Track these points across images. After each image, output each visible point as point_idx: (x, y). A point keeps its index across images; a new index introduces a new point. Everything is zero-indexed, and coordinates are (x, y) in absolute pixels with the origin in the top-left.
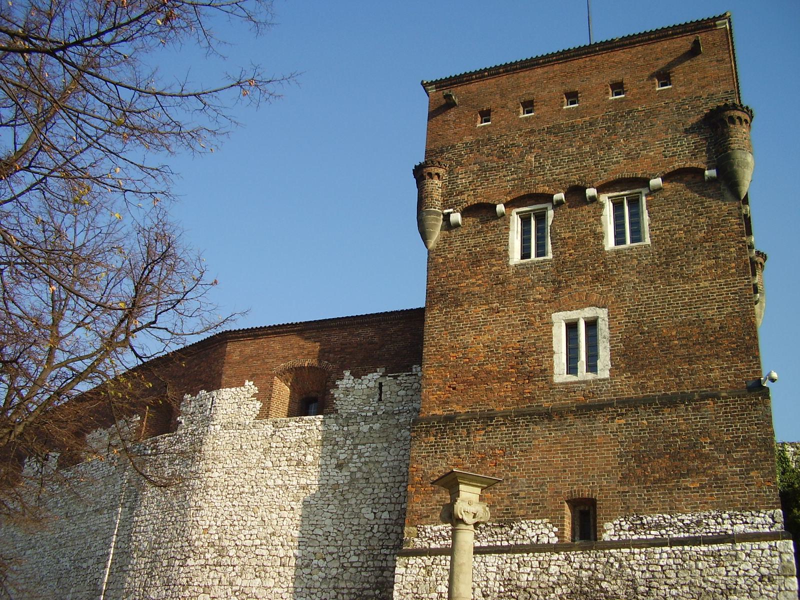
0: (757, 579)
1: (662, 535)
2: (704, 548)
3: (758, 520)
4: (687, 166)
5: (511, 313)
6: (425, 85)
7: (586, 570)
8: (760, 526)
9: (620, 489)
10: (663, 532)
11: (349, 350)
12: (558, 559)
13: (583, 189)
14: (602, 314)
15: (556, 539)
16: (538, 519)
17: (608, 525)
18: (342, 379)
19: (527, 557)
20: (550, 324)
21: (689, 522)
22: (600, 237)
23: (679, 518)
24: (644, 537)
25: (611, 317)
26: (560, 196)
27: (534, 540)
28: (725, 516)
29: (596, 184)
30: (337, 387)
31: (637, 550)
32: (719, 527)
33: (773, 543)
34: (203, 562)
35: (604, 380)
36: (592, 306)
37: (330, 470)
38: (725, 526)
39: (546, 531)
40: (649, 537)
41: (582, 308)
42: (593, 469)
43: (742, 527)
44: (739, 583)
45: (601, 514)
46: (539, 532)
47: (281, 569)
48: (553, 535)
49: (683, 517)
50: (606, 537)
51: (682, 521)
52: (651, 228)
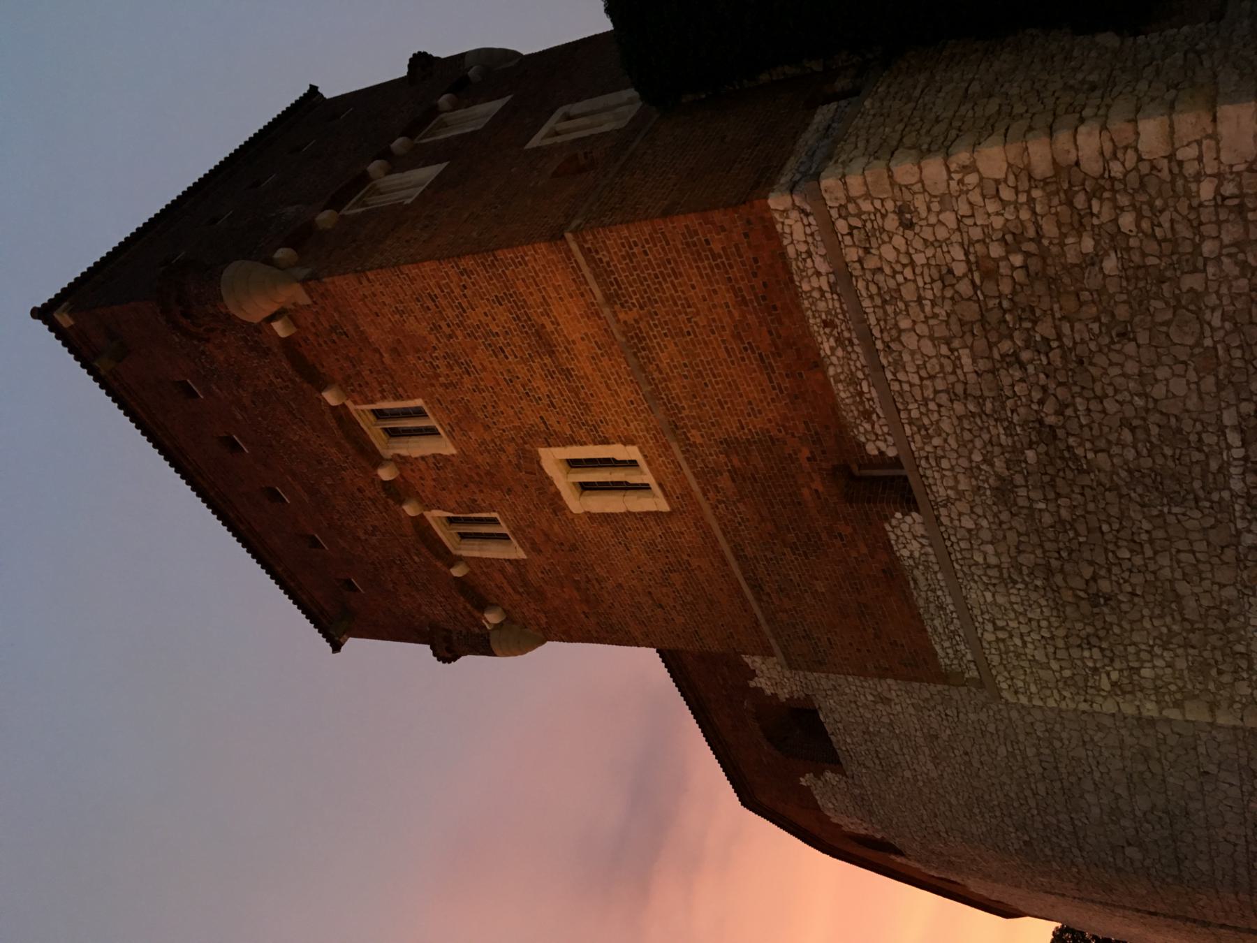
0: (909, 234)
1: (866, 377)
3: (799, 235)
6: (336, 648)
8: (808, 231)
10: (860, 375)
11: (721, 682)
12: (949, 516)
15: (914, 514)
16: (887, 535)
18: (762, 690)
21: (832, 340)
23: (829, 352)
24: (876, 400)
26: (410, 509)
27: (924, 541)
28: (806, 287)
30: (775, 695)
31: (903, 415)
32: (828, 295)
33: (834, 213)
34: (1076, 851)
35: (641, 450)
36: (541, 468)
37: (895, 712)
38: (826, 287)
39: (905, 527)
40: (874, 394)
41: (548, 478)
42: (784, 468)
43: (818, 260)
44: (924, 261)
46: (908, 536)
48: (908, 519)
49: (826, 346)
51: (832, 348)
52: (398, 397)
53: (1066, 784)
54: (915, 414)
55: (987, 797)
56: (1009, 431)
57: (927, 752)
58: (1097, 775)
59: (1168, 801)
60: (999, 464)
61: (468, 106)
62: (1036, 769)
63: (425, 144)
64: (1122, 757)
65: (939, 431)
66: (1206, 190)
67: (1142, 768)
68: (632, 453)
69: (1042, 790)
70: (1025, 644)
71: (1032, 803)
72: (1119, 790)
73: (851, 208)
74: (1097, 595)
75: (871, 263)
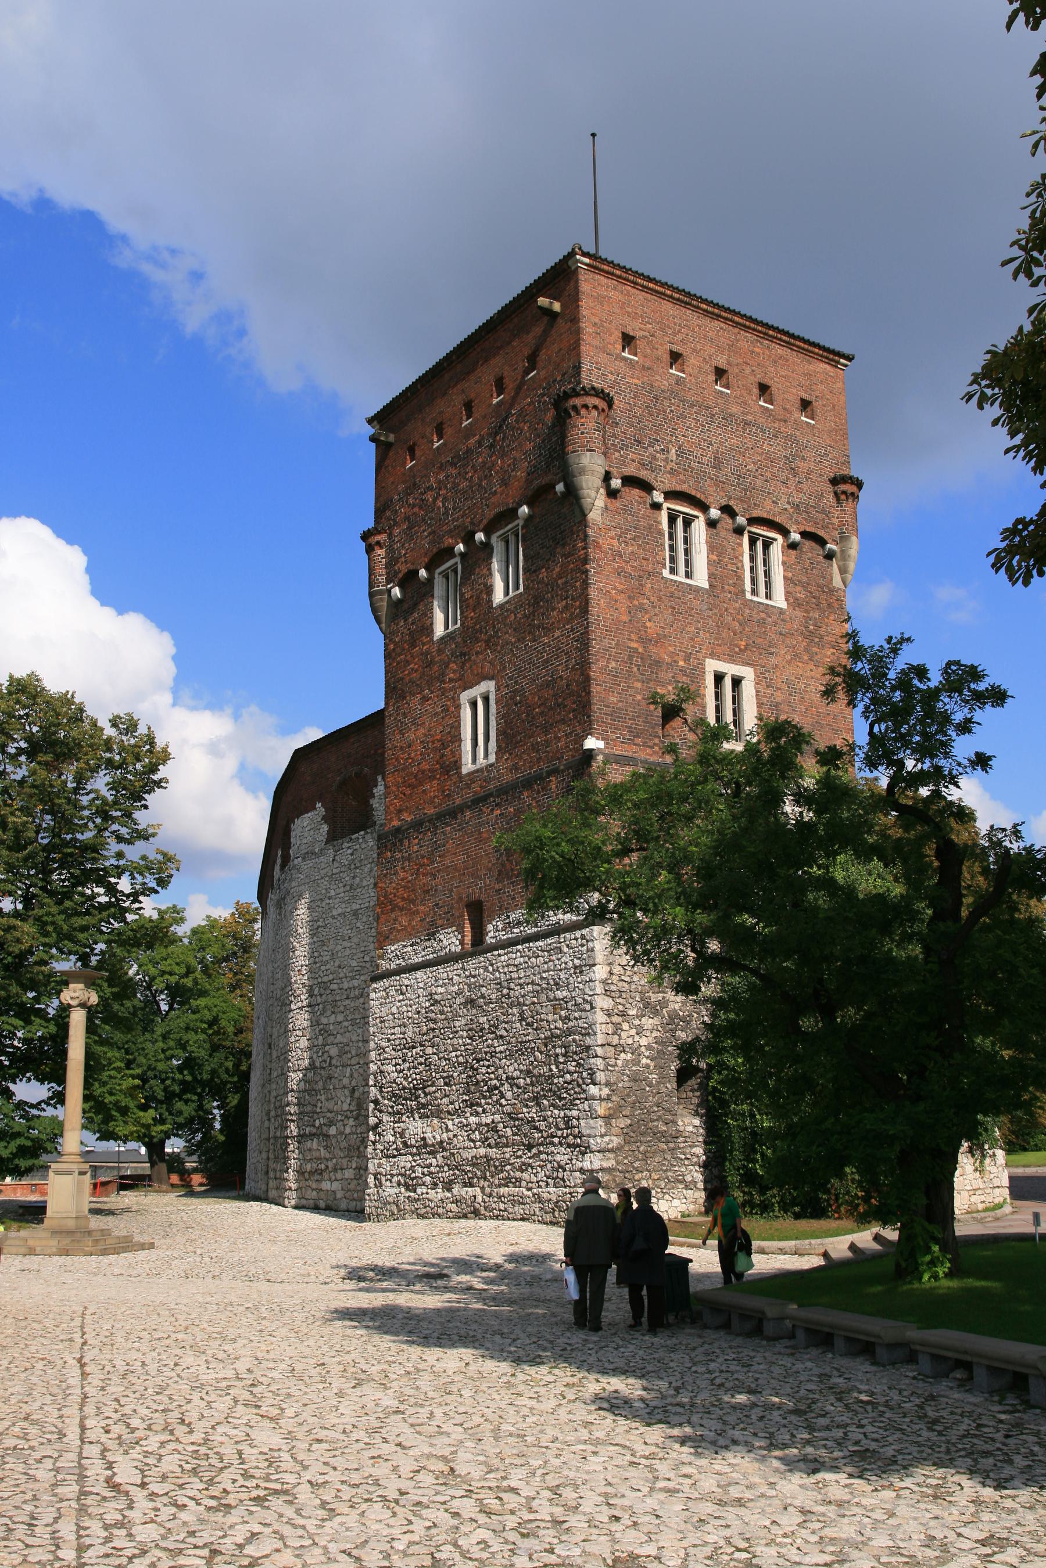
0: (572, 971)
2: (540, 943)
4: (543, 483)
5: (436, 699)
7: (474, 977)
9: (497, 887)
13: (473, 534)
14: (488, 686)
17: (490, 927)
18: (376, 786)
19: (441, 969)
20: (458, 707)
22: (489, 590)
25: (498, 689)
29: (482, 526)
31: (501, 952)
33: (584, 932)
41: (478, 683)
45: (485, 914)
47: (347, 1002)
50: (489, 939)
53: (339, 1003)
55: (325, 948)
57: (348, 910)
58: (346, 1024)
61: (784, 563)
62: (346, 986)
63: (741, 545)
64: (358, 1041)
66: (575, 1113)
67: (354, 1052)
68: (492, 758)
69: (334, 986)
71: (325, 979)
72: (339, 1036)
73: (584, 941)
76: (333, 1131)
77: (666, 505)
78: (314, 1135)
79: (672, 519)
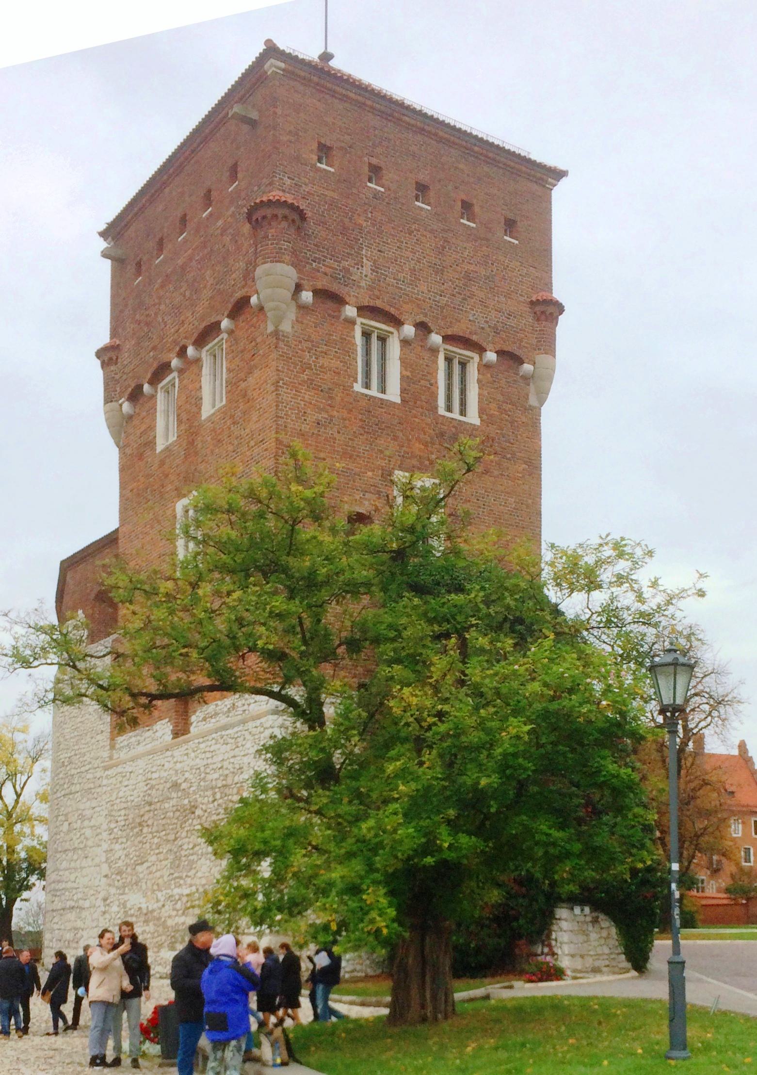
31: (201, 740)
54: (202, 746)
56: (195, 793)
59: (91, 847)
60: (184, 786)
65: (196, 757)
70: (126, 786)
74: (143, 826)
75: (248, 736)
76: (87, 904)
77: (359, 320)
78: (73, 908)
79: (366, 335)
